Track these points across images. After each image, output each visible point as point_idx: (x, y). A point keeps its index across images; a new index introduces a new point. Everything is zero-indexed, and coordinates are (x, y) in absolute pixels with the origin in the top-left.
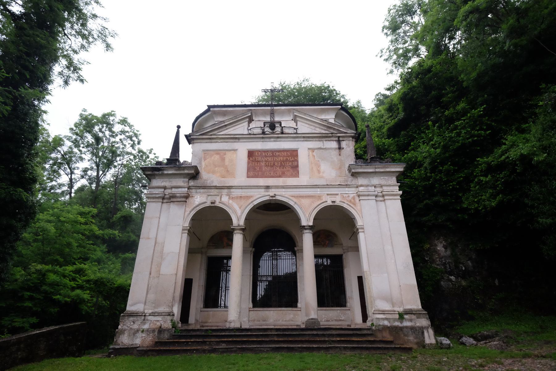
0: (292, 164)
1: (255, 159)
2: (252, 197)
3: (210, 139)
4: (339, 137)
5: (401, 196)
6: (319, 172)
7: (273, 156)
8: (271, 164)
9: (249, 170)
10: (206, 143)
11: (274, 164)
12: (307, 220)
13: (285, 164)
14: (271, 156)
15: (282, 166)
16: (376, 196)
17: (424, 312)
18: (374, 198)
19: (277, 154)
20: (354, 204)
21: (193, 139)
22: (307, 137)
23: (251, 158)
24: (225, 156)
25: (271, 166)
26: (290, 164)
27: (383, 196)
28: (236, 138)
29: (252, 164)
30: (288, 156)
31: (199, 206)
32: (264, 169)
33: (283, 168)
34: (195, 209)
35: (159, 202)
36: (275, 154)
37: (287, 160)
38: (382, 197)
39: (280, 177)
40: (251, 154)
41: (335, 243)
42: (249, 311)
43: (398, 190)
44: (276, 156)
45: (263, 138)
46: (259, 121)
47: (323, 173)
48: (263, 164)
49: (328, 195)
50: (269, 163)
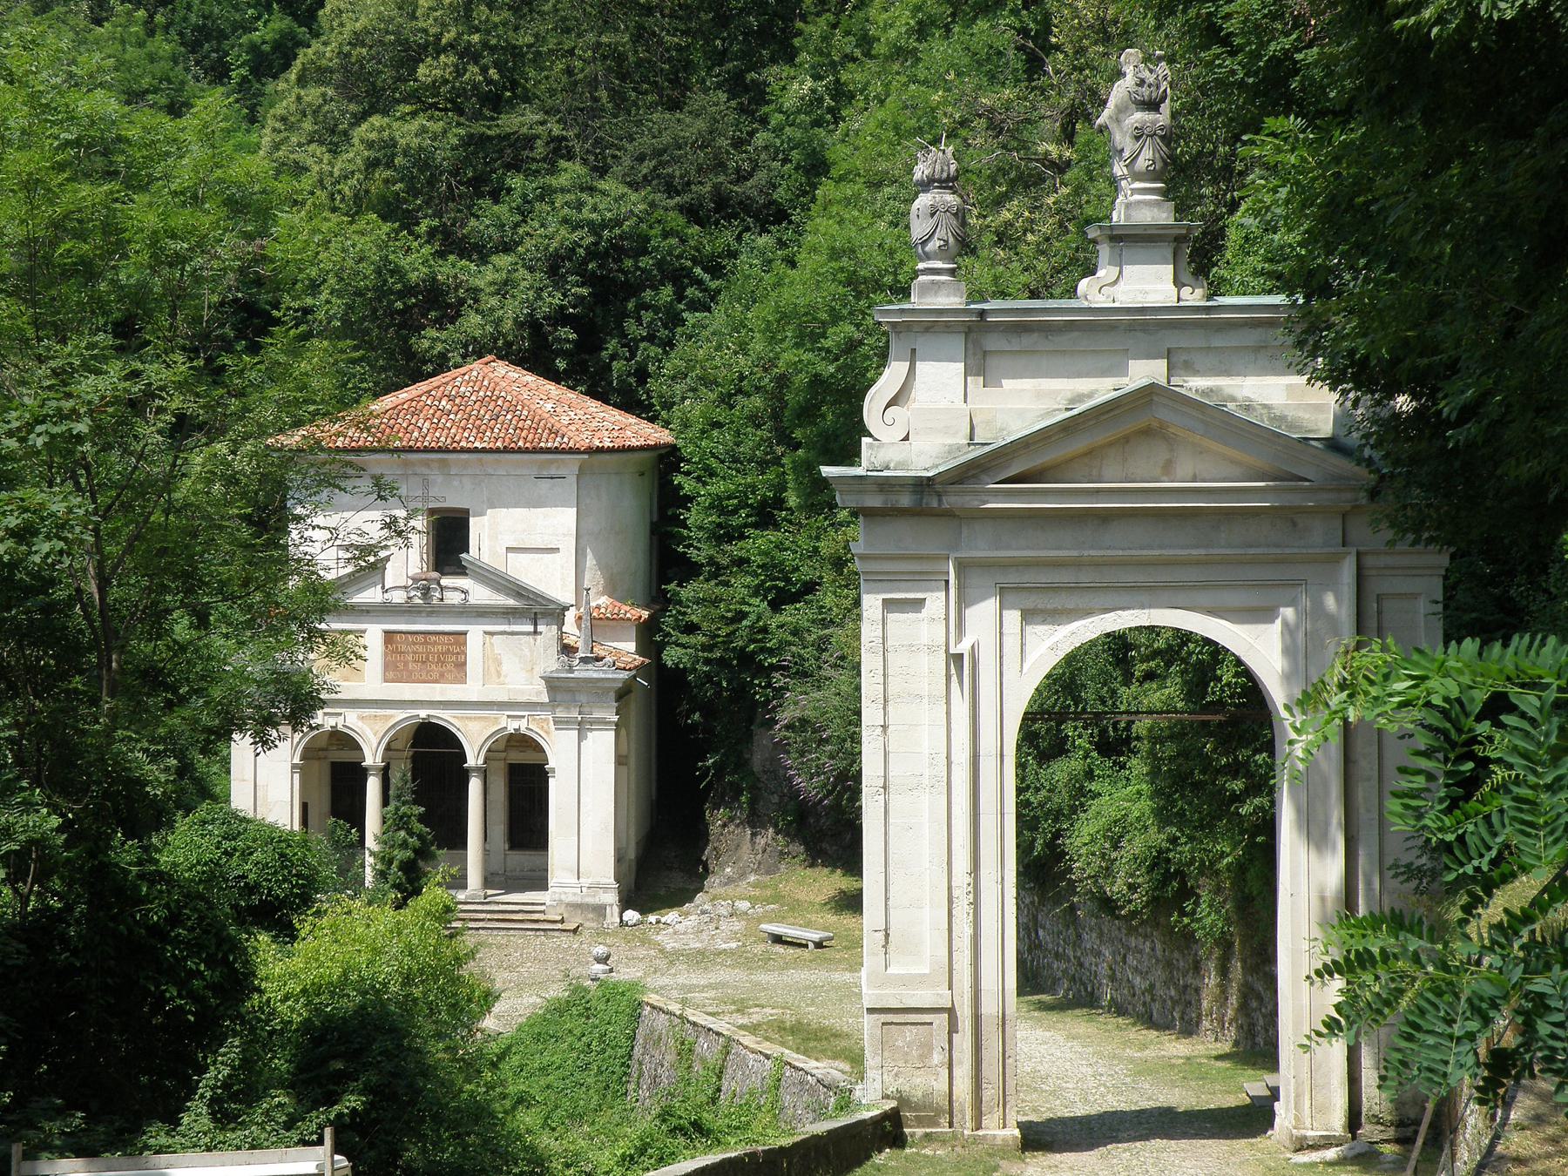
2: (391, 716)
6: (499, 674)
7: (426, 643)
9: (386, 667)
11: (427, 659)
15: (440, 662)
16: (579, 724)
19: (433, 638)
20: (547, 733)
25: (423, 662)
26: (454, 658)
47: (506, 676)
49: (508, 716)
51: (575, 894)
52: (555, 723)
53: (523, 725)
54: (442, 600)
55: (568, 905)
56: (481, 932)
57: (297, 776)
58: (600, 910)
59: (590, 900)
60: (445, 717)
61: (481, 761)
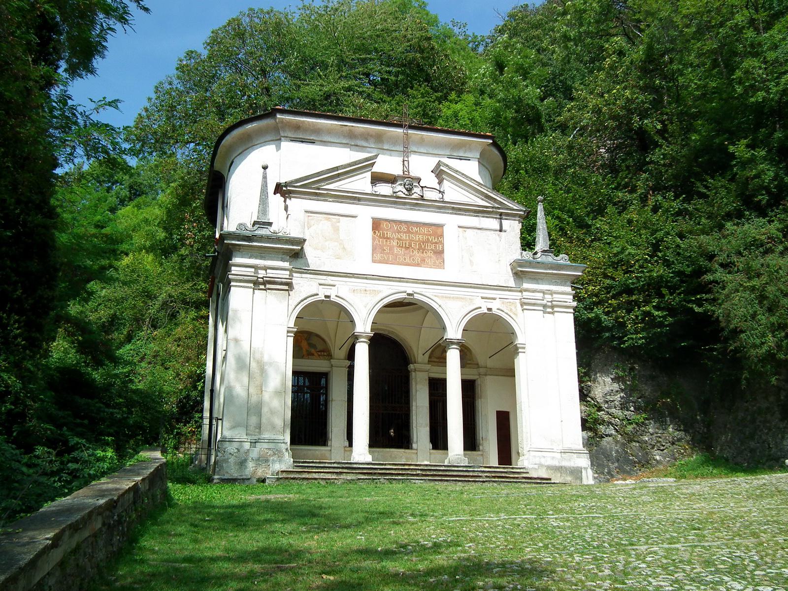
0: (436, 247)
1: (383, 234)
2: (380, 292)
3: (316, 194)
4: (501, 214)
5: (575, 309)
7: (408, 232)
8: (406, 244)
10: (310, 199)
12: (454, 332)
13: (425, 246)
14: (405, 232)
15: (421, 249)
17: (586, 452)
18: (542, 308)
21: (290, 192)
22: (458, 209)
23: (377, 232)
24: (338, 224)
25: (407, 248)
26: (433, 247)
27: (552, 307)
28: (355, 198)
29: (379, 242)
30: (430, 235)
31: (308, 300)
32: (396, 250)
33: (423, 253)
34: (302, 303)
35: (251, 288)
36: (412, 229)
37: (428, 241)
38: (550, 308)
39: (418, 265)
40: (377, 224)
41: (469, 362)
42: (345, 450)
43: (571, 301)
44: (412, 233)
45: (395, 203)
46: (357, 146)
48: (395, 244)
49: (482, 298)
50: (402, 243)
51: (553, 458)
52: (522, 304)
53: (495, 306)
54: (422, 196)
55: (549, 468)
56: (486, 484)
57: (291, 340)
58: (576, 473)
59: (565, 464)
60: (426, 294)
61: (459, 337)
